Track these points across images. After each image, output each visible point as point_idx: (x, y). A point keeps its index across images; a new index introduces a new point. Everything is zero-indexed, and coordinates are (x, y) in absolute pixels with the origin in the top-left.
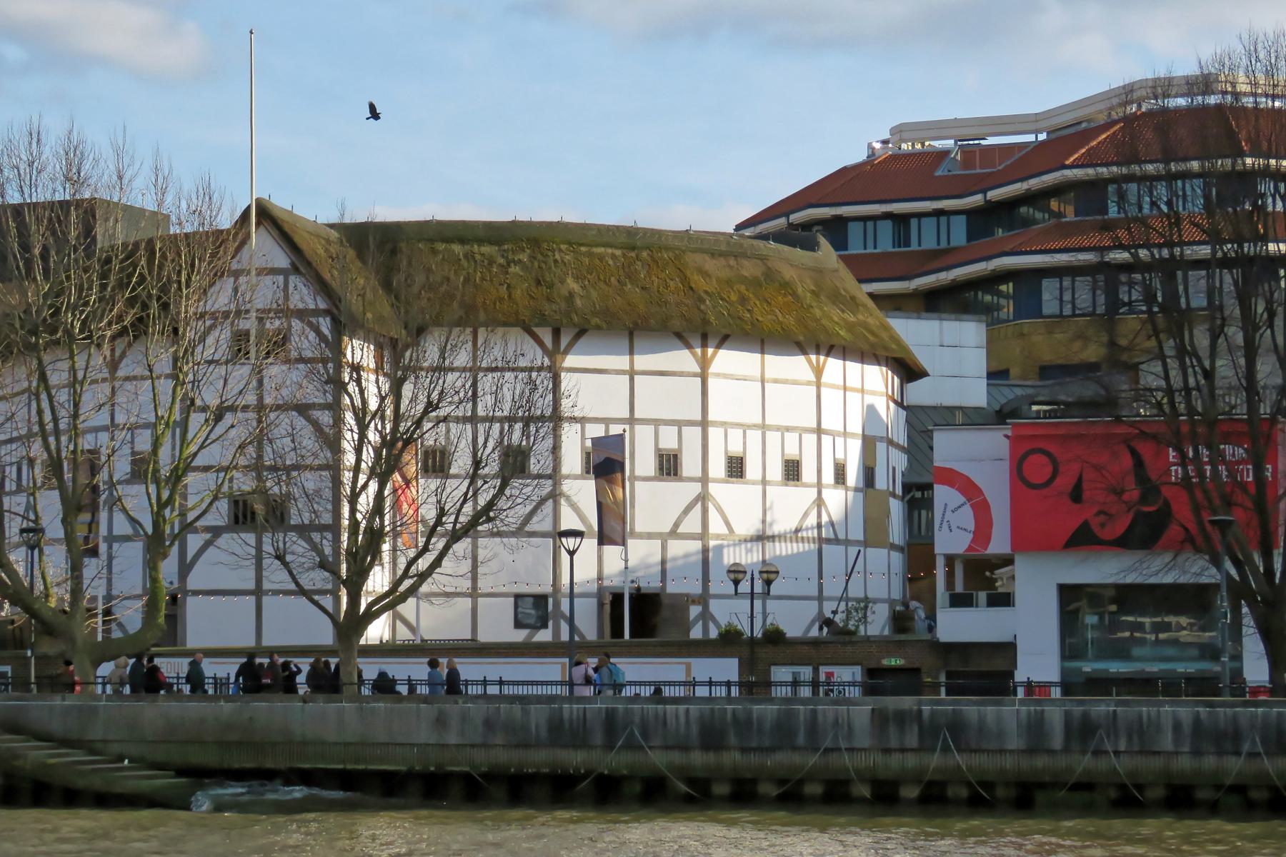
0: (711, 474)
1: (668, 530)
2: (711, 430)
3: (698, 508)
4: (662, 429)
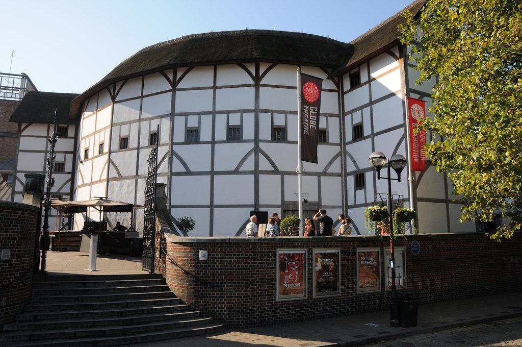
0: (261, 137)
1: (233, 169)
2: (261, 115)
3: (253, 156)
4: (230, 115)
